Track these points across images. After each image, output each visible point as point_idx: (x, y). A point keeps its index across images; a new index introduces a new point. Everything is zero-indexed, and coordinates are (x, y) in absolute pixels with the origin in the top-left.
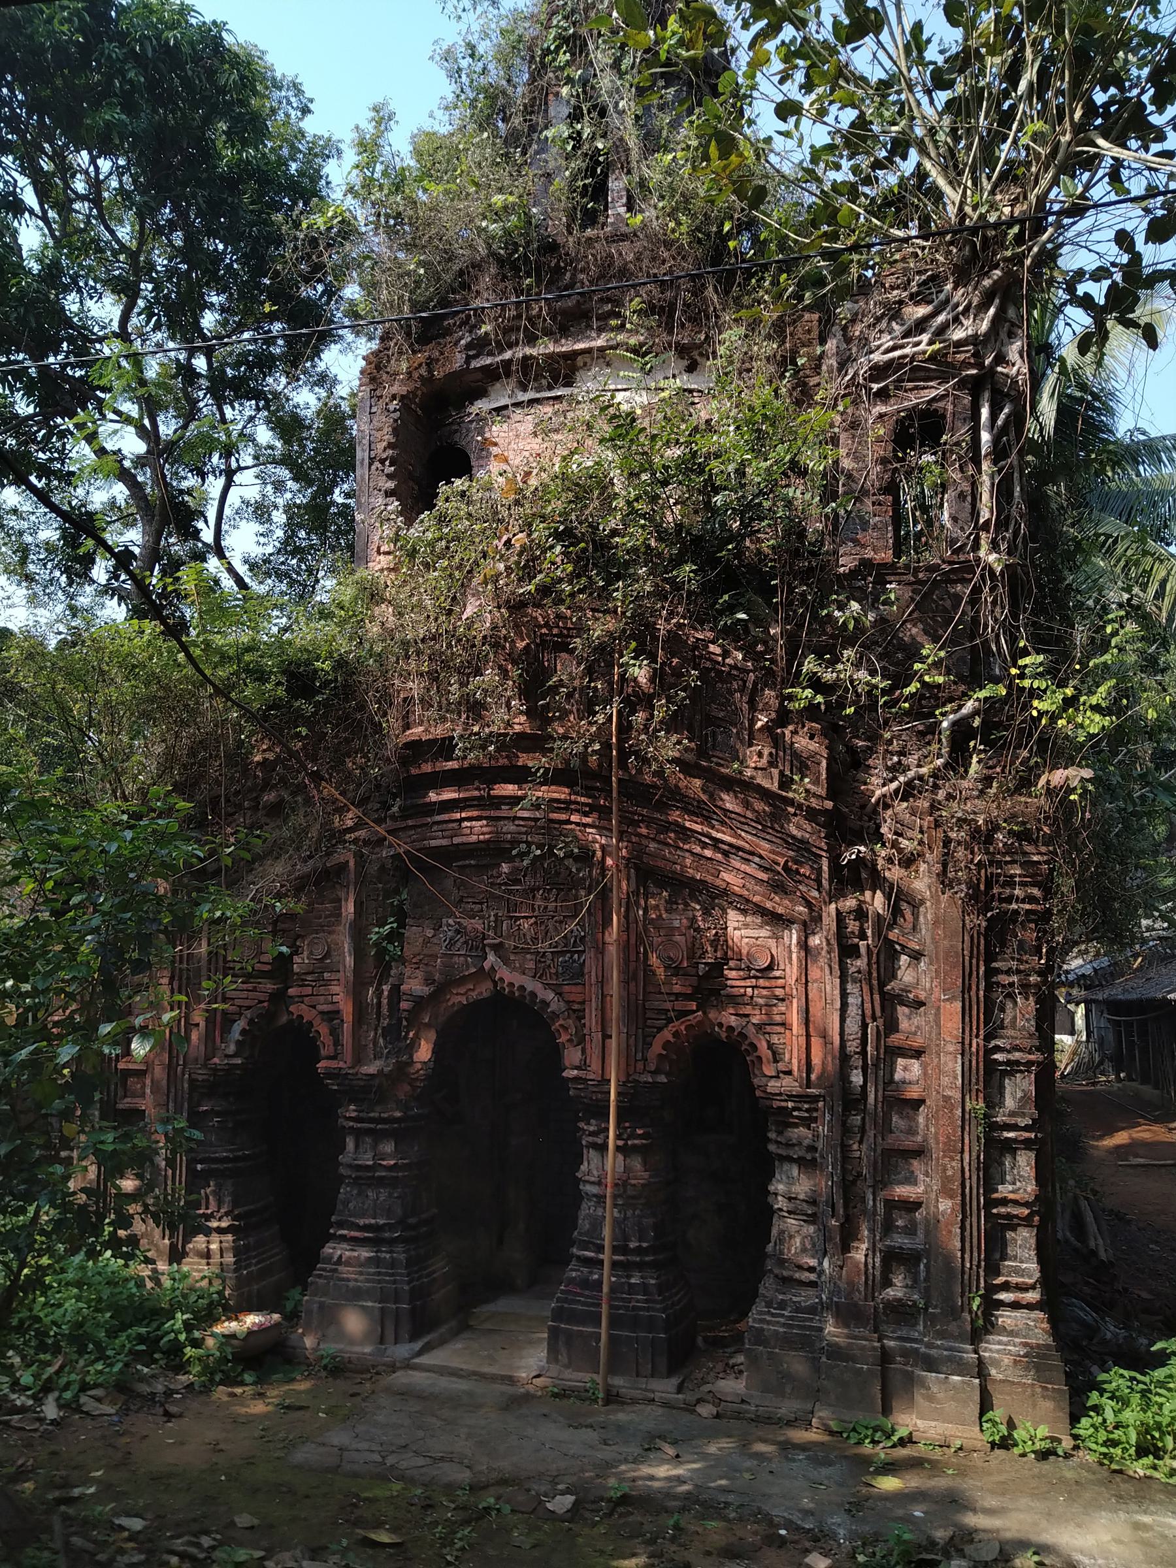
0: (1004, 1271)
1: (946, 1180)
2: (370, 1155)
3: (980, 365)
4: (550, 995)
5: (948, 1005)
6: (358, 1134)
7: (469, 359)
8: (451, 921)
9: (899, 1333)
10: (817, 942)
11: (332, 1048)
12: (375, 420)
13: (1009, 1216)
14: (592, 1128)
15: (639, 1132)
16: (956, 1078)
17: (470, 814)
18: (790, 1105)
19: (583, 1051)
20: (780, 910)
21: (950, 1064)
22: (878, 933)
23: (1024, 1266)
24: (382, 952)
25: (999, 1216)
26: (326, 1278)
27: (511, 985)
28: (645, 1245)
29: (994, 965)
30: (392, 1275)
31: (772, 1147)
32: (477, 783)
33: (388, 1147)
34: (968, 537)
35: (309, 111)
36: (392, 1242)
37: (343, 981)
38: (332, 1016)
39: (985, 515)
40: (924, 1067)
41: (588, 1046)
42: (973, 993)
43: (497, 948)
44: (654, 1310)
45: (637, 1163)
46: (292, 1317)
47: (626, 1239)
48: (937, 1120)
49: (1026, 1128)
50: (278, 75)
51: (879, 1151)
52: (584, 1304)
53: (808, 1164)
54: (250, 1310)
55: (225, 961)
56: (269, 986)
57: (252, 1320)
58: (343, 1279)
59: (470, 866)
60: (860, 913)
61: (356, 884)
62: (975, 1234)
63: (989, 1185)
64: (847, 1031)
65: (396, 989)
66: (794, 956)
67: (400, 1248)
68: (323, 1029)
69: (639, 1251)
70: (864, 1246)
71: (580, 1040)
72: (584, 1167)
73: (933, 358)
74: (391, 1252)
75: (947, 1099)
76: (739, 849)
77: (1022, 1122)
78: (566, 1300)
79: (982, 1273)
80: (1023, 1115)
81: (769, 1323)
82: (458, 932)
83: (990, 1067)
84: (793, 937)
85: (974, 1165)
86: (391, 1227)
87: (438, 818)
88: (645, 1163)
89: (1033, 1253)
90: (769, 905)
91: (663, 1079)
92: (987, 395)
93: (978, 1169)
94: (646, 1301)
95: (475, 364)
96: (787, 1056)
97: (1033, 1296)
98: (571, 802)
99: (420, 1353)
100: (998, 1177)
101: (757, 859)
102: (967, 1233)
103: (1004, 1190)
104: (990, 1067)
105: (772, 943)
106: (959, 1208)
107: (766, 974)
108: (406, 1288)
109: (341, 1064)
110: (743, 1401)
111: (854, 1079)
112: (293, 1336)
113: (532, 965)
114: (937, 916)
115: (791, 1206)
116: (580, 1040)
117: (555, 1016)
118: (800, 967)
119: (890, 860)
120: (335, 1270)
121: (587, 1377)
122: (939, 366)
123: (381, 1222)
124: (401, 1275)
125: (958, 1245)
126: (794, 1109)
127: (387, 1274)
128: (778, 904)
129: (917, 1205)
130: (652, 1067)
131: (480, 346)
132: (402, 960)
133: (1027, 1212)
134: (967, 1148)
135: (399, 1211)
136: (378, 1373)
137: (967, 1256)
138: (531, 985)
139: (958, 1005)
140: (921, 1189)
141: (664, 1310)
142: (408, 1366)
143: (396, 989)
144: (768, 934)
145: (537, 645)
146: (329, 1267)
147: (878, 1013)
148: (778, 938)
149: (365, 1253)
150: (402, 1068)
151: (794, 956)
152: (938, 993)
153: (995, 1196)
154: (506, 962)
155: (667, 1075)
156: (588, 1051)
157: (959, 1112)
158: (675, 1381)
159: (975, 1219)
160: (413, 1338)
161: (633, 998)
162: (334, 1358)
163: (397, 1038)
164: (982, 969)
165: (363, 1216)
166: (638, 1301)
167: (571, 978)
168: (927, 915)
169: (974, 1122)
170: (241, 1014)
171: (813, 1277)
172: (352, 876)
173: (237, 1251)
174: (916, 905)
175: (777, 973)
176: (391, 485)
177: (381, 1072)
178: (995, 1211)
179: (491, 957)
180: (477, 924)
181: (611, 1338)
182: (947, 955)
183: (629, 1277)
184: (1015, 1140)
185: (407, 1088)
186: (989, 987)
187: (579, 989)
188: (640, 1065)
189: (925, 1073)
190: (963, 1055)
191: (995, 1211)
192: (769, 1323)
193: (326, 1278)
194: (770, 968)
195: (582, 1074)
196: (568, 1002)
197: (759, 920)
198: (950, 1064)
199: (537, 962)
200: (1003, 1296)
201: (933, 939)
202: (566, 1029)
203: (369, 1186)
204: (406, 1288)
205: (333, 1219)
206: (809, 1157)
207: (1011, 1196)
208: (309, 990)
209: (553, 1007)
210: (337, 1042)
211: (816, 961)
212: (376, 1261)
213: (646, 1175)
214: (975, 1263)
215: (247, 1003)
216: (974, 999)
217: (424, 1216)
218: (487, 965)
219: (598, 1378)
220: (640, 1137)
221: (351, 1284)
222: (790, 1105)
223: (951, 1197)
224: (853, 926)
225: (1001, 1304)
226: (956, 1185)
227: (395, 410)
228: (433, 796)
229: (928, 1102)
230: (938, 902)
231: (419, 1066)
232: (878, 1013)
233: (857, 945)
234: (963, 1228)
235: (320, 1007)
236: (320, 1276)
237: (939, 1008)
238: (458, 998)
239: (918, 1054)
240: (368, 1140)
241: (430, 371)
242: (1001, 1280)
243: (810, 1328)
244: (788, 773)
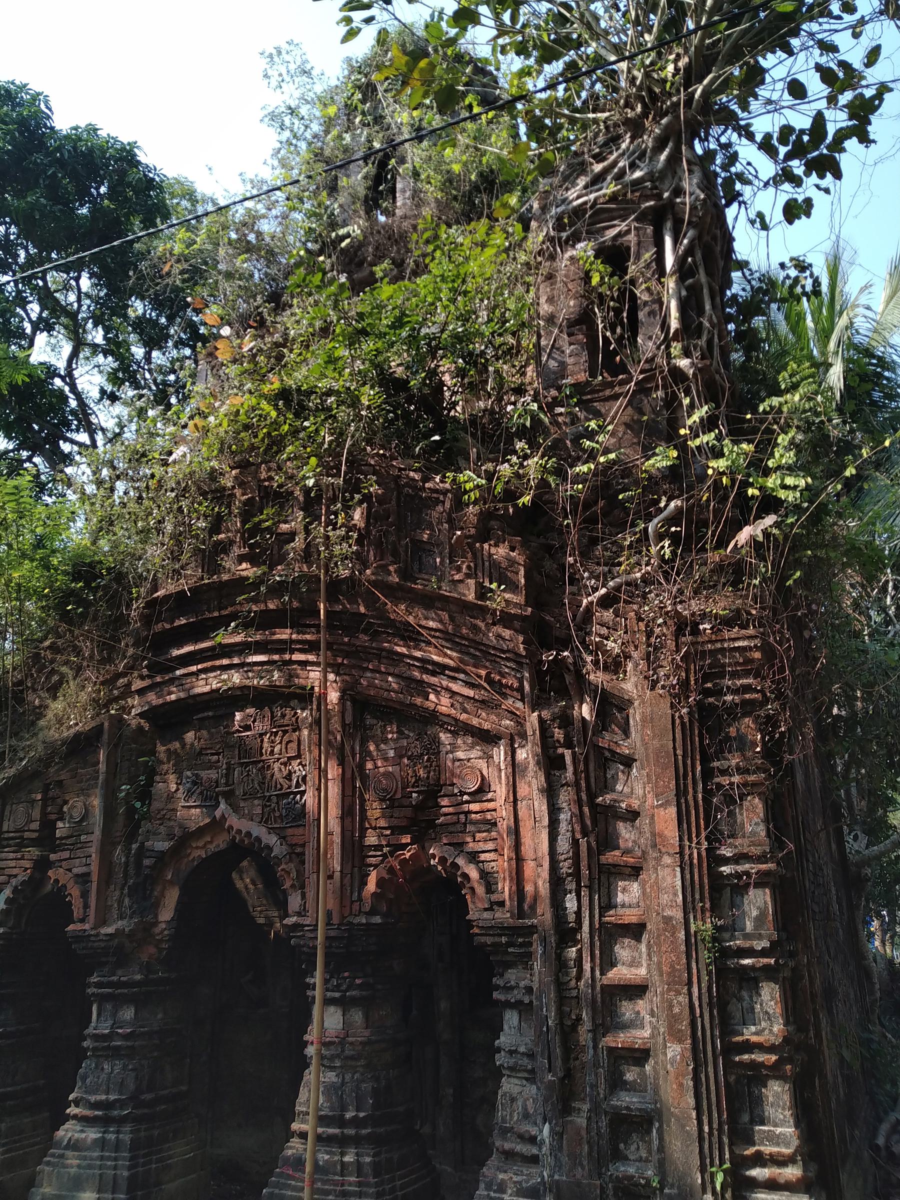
1: (673, 1020)
3: (659, 197)
4: (272, 840)
5: (662, 812)
10: (524, 755)
13: (753, 1065)
15: (358, 981)
16: (675, 894)
18: (504, 940)
19: (303, 896)
20: (486, 726)
21: (669, 880)
23: (779, 1130)
24: (131, 810)
27: (239, 832)
30: (116, 1159)
31: (496, 995)
33: (128, 1014)
36: (121, 1121)
39: (674, 324)
42: (690, 797)
43: (229, 796)
47: (344, 1108)
48: (659, 945)
49: (764, 953)
51: (598, 988)
56: (34, 852)
59: (208, 718)
60: (565, 720)
61: (109, 744)
62: (713, 1088)
68: (75, 892)
69: (356, 1122)
70: (586, 1107)
75: (668, 920)
76: (445, 667)
77: (759, 945)
79: (726, 1140)
80: (760, 937)
82: (194, 783)
83: (717, 883)
84: (500, 754)
85: (705, 999)
86: (121, 1104)
87: (178, 673)
88: (367, 1017)
89: (788, 1113)
90: (475, 722)
91: (377, 920)
92: (669, 224)
93: (710, 1004)
94: (359, 1184)
96: (500, 886)
97: (792, 1172)
98: (292, 641)
100: (738, 1015)
101: (462, 676)
103: (749, 1033)
104: (717, 883)
105: (482, 764)
106: (689, 1054)
107: (478, 797)
111: (568, 905)
115: (512, 1061)
117: (279, 861)
118: (507, 784)
119: (596, 663)
120: (62, 1156)
122: (619, 206)
123: (112, 1097)
125: (692, 1102)
126: (509, 944)
128: (484, 721)
130: (367, 908)
133: (774, 1058)
135: (131, 1086)
137: (705, 1119)
138: (258, 831)
139: (673, 810)
140: (647, 1033)
145: (261, 498)
149: (92, 1134)
150: (147, 929)
152: (651, 800)
154: (236, 809)
155: (384, 916)
157: (682, 935)
159: (711, 1069)
161: (348, 834)
163: (144, 896)
164: (699, 768)
166: (350, 1184)
167: (294, 820)
168: (636, 716)
174: (624, 705)
175: (490, 796)
180: (213, 774)
183: (343, 1154)
184: (752, 968)
185: (152, 950)
186: (708, 794)
187: (300, 831)
189: (644, 893)
195: (301, 920)
197: (470, 740)
198: (669, 880)
199: (264, 806)
200: (756, 1172)
201: (643, 740)
203: (107, 1057)
204: (126, 1174)
206: (526, 1000)
207: (754, 1039)
208: (66, 854)
211: (523, 776)
212: (101, 1143)
213: (367, 1033)
214: (715, 1126)
215: (15, 871)
216: (692, 803)
218: (218, 814)
223: (680, 1041)
224: (558, 734)
225: (754, 1184)
226: (684, 1025)
228: (176, 652)
229: (649, 927)
231: (164, 926)
235: (75, 871)
236: (48, 1163)
237: (652, 817)
238: (198, 852)
239: (635, 872)
240: (109, 1007)
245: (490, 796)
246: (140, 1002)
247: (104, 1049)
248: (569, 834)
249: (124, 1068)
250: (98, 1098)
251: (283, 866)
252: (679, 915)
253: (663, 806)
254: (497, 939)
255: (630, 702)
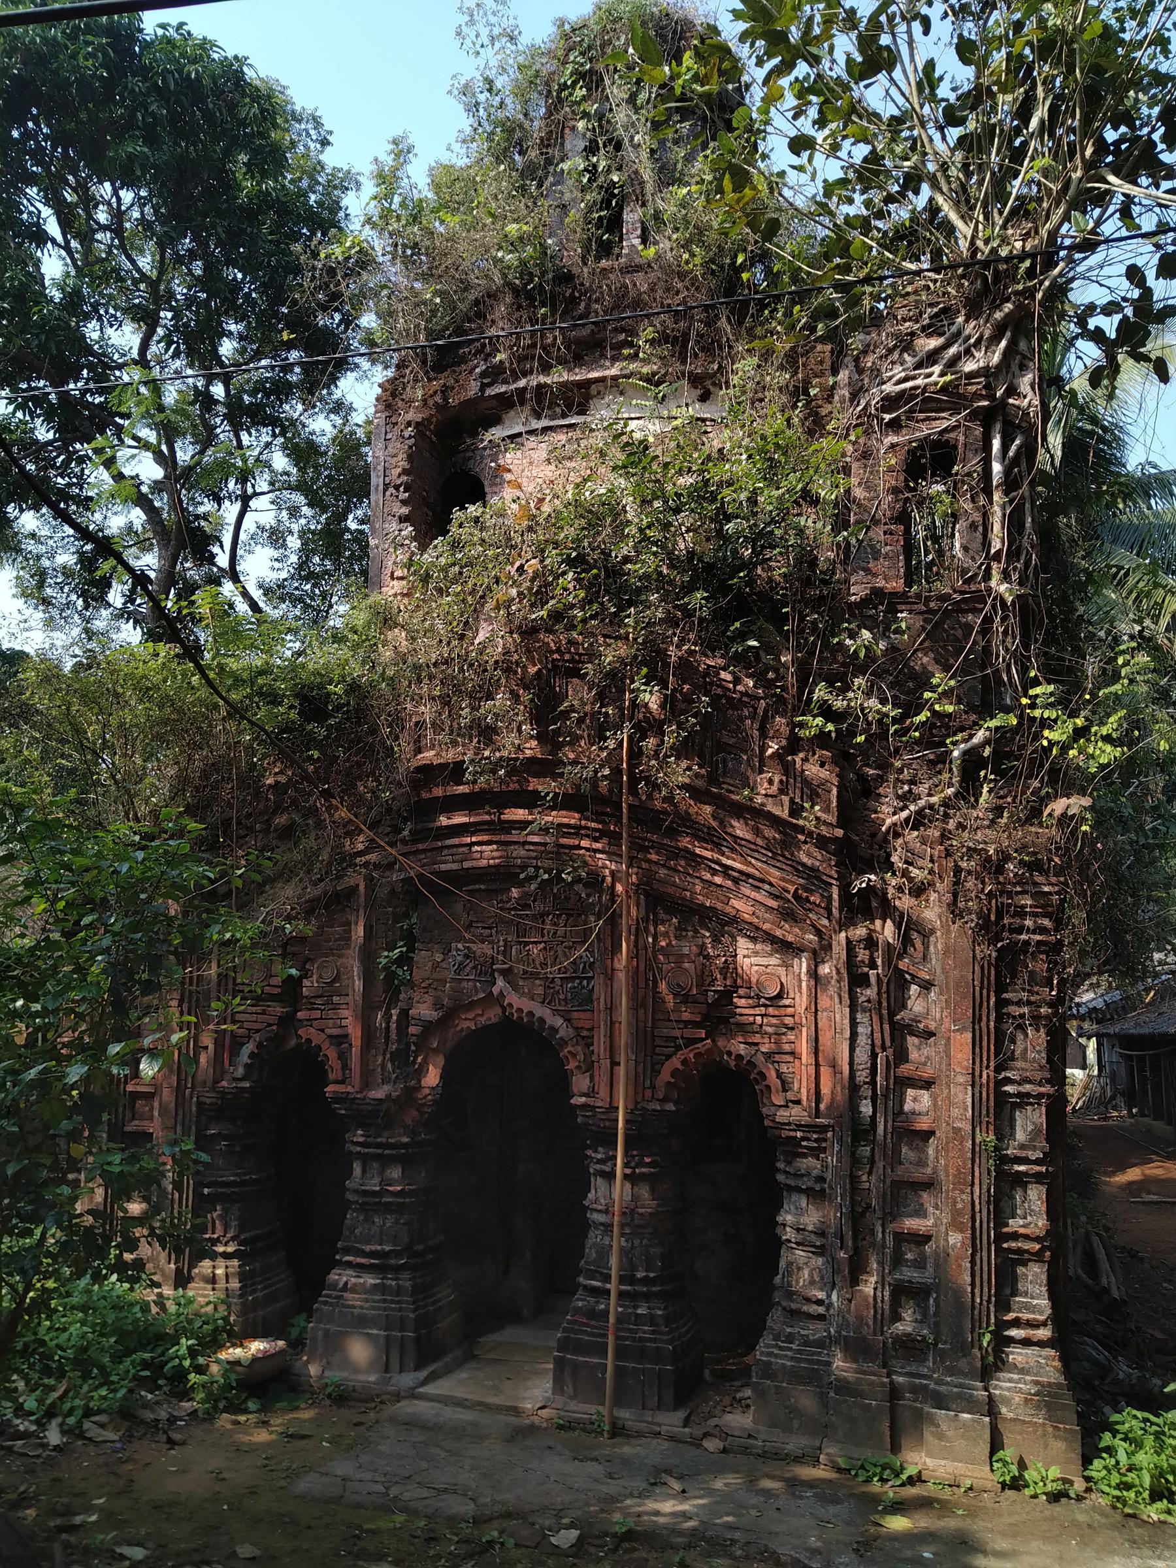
0: (1015, 1307)
1: (956, 1213)
2: (376, 1180)
3: (991, 397)
4: (558, 1022)
6: (365, 1159)
7: (484, 386)
8: (460, 946)
9: (908, 1369)
10: (827, 970)
11: (340, 1073)
12: (390, 446)
13: (1020, 1251)
14: (599, 1156)
15: (647, 1160)
17: (480, 838)
18: (799, 1134)
19: (592, 1078)
20: (790, 938)
21: (961, 1096)
22: (888, 962)
23: (1035, 1302)
24: (391, 976)
25: (1009, 1250)
26: (331, 1304)
27: (520, 1010)
28: (652, 1275)
29: (1005, 995)
30: (398, 1302)
31: (780, 1178)
32: (487, 808)
33: (395, 1173)
34: (979, 568)
35: (329, 143)
36: (398, 1269)
37: (352, 1004)
38: (341, 1040)
39: (996, 545)
40: (934, 1098)
41: (596, 1073)
42: (983, 1024)
43: (506, 973)
44: (661, 1341)
45: (644, 1192)
46: (297, 1344)
47: (634, 1269)
48: (947, 1151)
49: (1037, 1162)
50: (298, 108)
52: (590, 1334)
53: (817, 1195)
54: (255, 1336)
55: (235, 984)
56: (278, 1009)
57: (257, 1346)
58: (349, 1307)
59: (480, 890)
60: (870, 942)
62: (985, 1268)
63: (1000, 1220)
64: (857, 1060)
65: (404, 1014)
66: (804, 984)
67: (405, 1275)
68: (332, 1053)
69: (646, 1281)
70: (873, 1279)
71: (589, 1067)
72: (591, 1195)
73: (944, 389)
74: (397, 1279)
75: (957, 1131)
76: (749, 876)
77: (1034, 1155)
78: (572, 1330)
79: (992, 1309)
80: (1034, 1148)
81: (776, 1356)
82: (467, 957)
83: (1001, 1099)
84: (802, 965)
85: (985, 1198)
86: (397, 1254)
87: (448, 842)
88: (653, 1191)
89: (1044, 1289)
90: (778, 933)
91: (671, 1107)
92: (998, 426)
93: (988, 1202)
94: (653, 1332)
95: (490, 392)
96: (796, 1086)
97: (1044, 1333)
98: (581, 827)
99: (424, 1383)
100: (1009, 1210)
101: (767, 887)
102: (977, 1268)
103: (1015, 1225)
104: (1001, 1099)
105: (782, 971)
106: (969, 1242)
108: (412, 1315)
109: (349, 1089)
110: (750, 1436)
111: (863, 1109)
112: (298, 1364)
113: (540, 991)
114: (947, 948)
115: (800, 1237)
116: (589, 1067)
117: (563, 1042)
118: (809, 996)
119: (900, 889)
121: (593, 1409)
122: (950, 397)
123: (387, 1248)
124: (407, 1302)
125: (968, 1279)
127: (392, 1302)
129: (927, 1238)
131: (495, 374)
132: (411, 984)
133: (1038, 1247)
134: (977, 1181)
135: (406, 1239)
136: (382, 1402)
137: (977, 1291)
138: (540, 1011)
139: (968, 1036)
140: (930, 1222)
141: (670, 1342)
142: (412, 1395)
143: (404, 1014)
144: (777, 962)
145: (549, 670)
146: (334, 1293)
147: (888, 1043)
148: (787, 966)
149: (371, 1280)
150: (411, 1093)
151: (804, 984)
152: (947, 1023)
153: (1005, 1230)
154: (516, 988)
155: (676, 1103)
156: (596, 1078)
157: (969, 1144)
158: (681, 1414)
159: (985, 1254)
160: (417, 1368)
161: (641, 1024)
162: (338, 1386)
163: (406, 1065)
164: (993, 1000)
165: (368, 1242)
167: (580, 1005)
168: (937, 944)
169: (984, 1155)
170: (249, 1037)
171: (821, 1310)
172: (362, 899)
173: (242, 1277)
174: (926, 934)
175: (786, 1002)
176: (405, 510)
177: (388, 1096)
178: (1005, 1245)
179: (500, 983)
180: (486, 949)
181: (619, 1371)
182: (957, 985)
183: (636, 1307)
184: (1025, 1174)
185: (415, 1113)
186: (999, 1019)
187: (588, 1015)
188: (648, 1093)
189: (935, 1104)
190: (973, 1086)
191: (1005, 1245)
192: (776, 1356)
193: (331, 1304)
194: (780, 996)
195: (590, 1101)
196: (576, 1029)
198: (961, 1096)
199: (546, 988)
200: (1013, 1332)
201: (943, 969)
202: (574, 1055)
204: (412, 1315)
205: (340, 1244)
207: (1022, 1231)
208: (317, 1014)
209: (562, 1033)
210: (345, 1066)
212: (381, 1289)
214: (985, 1298)
215: (256, 1026)
216: (984, 1030)
217: (431, 1243)
219: (604, 1410)
220: (648, 1165)
221: (357, 1311)
222: (799, 1134)
223: (962, 1231)
224: (863, 955)
225: (1011, 1341)
227: (410, 437)
228: (444, 821)
230: (948, 931)
231: (427, 1091)
232: (888, 1043)
233: (867, 974)
234: (973, 1262)
235: (328, 1031)
236: (325, 1303)
238: (467, 1023)
239: (928, 1084)
241: (445, 399)
242: (1011, 1316)
243: (818, 1362)
244: (798, 800)
245: (786, 1002)
246: (405, 1162)
247: (375, 1204)
248: (869, 1047)
249: (397, 1221)
250: (373, 1248)
251: (570, 1048)
252: (969, 1128)
253: (961, 1030)
254: (792, 1134)
255: (932, 931)
